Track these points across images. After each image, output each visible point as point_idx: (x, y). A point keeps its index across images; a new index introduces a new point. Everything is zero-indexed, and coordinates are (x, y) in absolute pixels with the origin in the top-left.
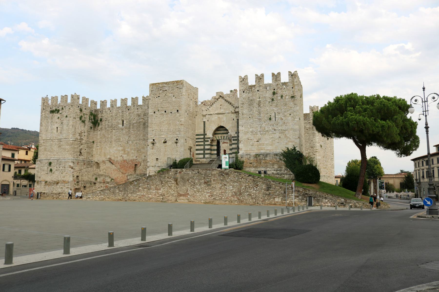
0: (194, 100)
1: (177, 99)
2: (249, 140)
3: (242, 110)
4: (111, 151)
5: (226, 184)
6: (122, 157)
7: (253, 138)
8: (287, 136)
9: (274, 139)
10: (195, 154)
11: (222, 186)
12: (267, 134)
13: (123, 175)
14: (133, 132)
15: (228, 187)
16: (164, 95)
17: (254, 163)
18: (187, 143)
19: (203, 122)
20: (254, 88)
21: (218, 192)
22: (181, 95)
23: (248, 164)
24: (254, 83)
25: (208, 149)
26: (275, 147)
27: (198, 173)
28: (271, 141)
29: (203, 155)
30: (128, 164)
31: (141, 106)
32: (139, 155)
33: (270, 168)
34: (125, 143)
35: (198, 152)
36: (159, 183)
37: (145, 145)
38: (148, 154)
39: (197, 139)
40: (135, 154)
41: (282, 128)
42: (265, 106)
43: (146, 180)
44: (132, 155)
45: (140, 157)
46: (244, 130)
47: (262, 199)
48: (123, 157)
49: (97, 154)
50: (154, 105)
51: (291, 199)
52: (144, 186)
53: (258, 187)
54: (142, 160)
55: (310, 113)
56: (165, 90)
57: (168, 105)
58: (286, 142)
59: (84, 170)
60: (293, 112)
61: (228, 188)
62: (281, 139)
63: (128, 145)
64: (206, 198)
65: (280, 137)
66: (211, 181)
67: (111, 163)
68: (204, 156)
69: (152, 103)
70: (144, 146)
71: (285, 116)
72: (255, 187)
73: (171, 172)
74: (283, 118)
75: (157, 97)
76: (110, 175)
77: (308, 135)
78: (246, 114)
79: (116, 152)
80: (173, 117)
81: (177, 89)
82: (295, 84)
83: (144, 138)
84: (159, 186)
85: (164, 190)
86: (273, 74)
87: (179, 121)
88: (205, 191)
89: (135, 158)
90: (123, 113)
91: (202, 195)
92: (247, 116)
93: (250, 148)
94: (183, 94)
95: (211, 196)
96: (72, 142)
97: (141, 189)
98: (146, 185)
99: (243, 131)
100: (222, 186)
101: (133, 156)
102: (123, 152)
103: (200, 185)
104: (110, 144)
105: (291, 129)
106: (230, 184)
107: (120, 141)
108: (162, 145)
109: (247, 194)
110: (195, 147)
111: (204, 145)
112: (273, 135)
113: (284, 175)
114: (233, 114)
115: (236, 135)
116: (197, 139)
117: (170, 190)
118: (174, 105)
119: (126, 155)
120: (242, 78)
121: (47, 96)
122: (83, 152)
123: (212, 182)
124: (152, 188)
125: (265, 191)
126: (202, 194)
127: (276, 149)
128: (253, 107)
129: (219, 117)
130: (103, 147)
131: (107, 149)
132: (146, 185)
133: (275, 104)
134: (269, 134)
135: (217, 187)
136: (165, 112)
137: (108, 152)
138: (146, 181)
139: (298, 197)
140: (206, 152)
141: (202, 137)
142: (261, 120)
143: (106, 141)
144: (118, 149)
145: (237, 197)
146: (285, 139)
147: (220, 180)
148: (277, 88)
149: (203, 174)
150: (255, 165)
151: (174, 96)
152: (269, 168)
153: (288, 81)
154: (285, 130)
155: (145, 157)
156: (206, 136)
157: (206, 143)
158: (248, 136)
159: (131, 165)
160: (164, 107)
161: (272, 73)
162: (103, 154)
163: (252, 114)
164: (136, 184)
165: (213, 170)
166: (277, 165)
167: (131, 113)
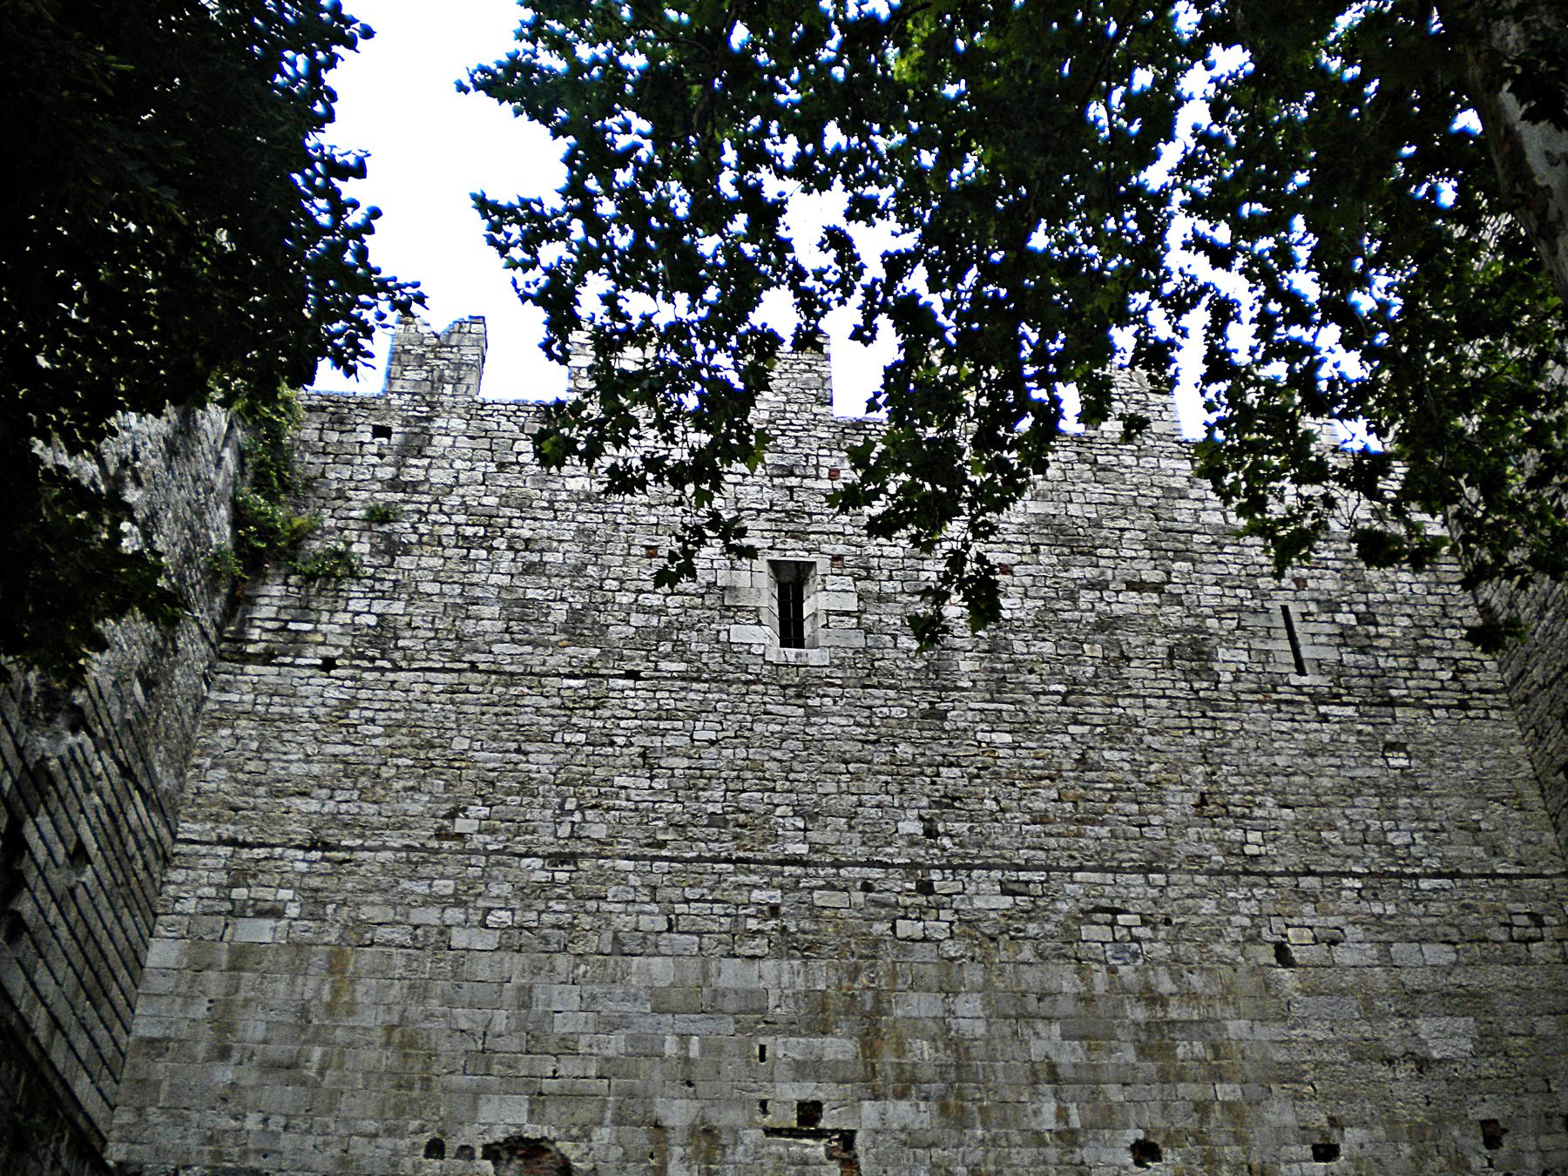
6: (817, 1149)
14: (1008, 738)
34: (867, 887)
40: (1115, 1093)
44: (1049, 1108)
45: (1231, 1152)
48: (847, 1138)
49: (224, 1053)
63: (939, 929)
70: (1256, 970)
79: (671, 1047)
90: (791, 489)
101: (1069, 1138)
102: (839, 1047)
104: (529, 893)
107: (769, 851)
130: (383, 933)
131: (483, 968)
137: (501, 1020)
143: (461, 825)
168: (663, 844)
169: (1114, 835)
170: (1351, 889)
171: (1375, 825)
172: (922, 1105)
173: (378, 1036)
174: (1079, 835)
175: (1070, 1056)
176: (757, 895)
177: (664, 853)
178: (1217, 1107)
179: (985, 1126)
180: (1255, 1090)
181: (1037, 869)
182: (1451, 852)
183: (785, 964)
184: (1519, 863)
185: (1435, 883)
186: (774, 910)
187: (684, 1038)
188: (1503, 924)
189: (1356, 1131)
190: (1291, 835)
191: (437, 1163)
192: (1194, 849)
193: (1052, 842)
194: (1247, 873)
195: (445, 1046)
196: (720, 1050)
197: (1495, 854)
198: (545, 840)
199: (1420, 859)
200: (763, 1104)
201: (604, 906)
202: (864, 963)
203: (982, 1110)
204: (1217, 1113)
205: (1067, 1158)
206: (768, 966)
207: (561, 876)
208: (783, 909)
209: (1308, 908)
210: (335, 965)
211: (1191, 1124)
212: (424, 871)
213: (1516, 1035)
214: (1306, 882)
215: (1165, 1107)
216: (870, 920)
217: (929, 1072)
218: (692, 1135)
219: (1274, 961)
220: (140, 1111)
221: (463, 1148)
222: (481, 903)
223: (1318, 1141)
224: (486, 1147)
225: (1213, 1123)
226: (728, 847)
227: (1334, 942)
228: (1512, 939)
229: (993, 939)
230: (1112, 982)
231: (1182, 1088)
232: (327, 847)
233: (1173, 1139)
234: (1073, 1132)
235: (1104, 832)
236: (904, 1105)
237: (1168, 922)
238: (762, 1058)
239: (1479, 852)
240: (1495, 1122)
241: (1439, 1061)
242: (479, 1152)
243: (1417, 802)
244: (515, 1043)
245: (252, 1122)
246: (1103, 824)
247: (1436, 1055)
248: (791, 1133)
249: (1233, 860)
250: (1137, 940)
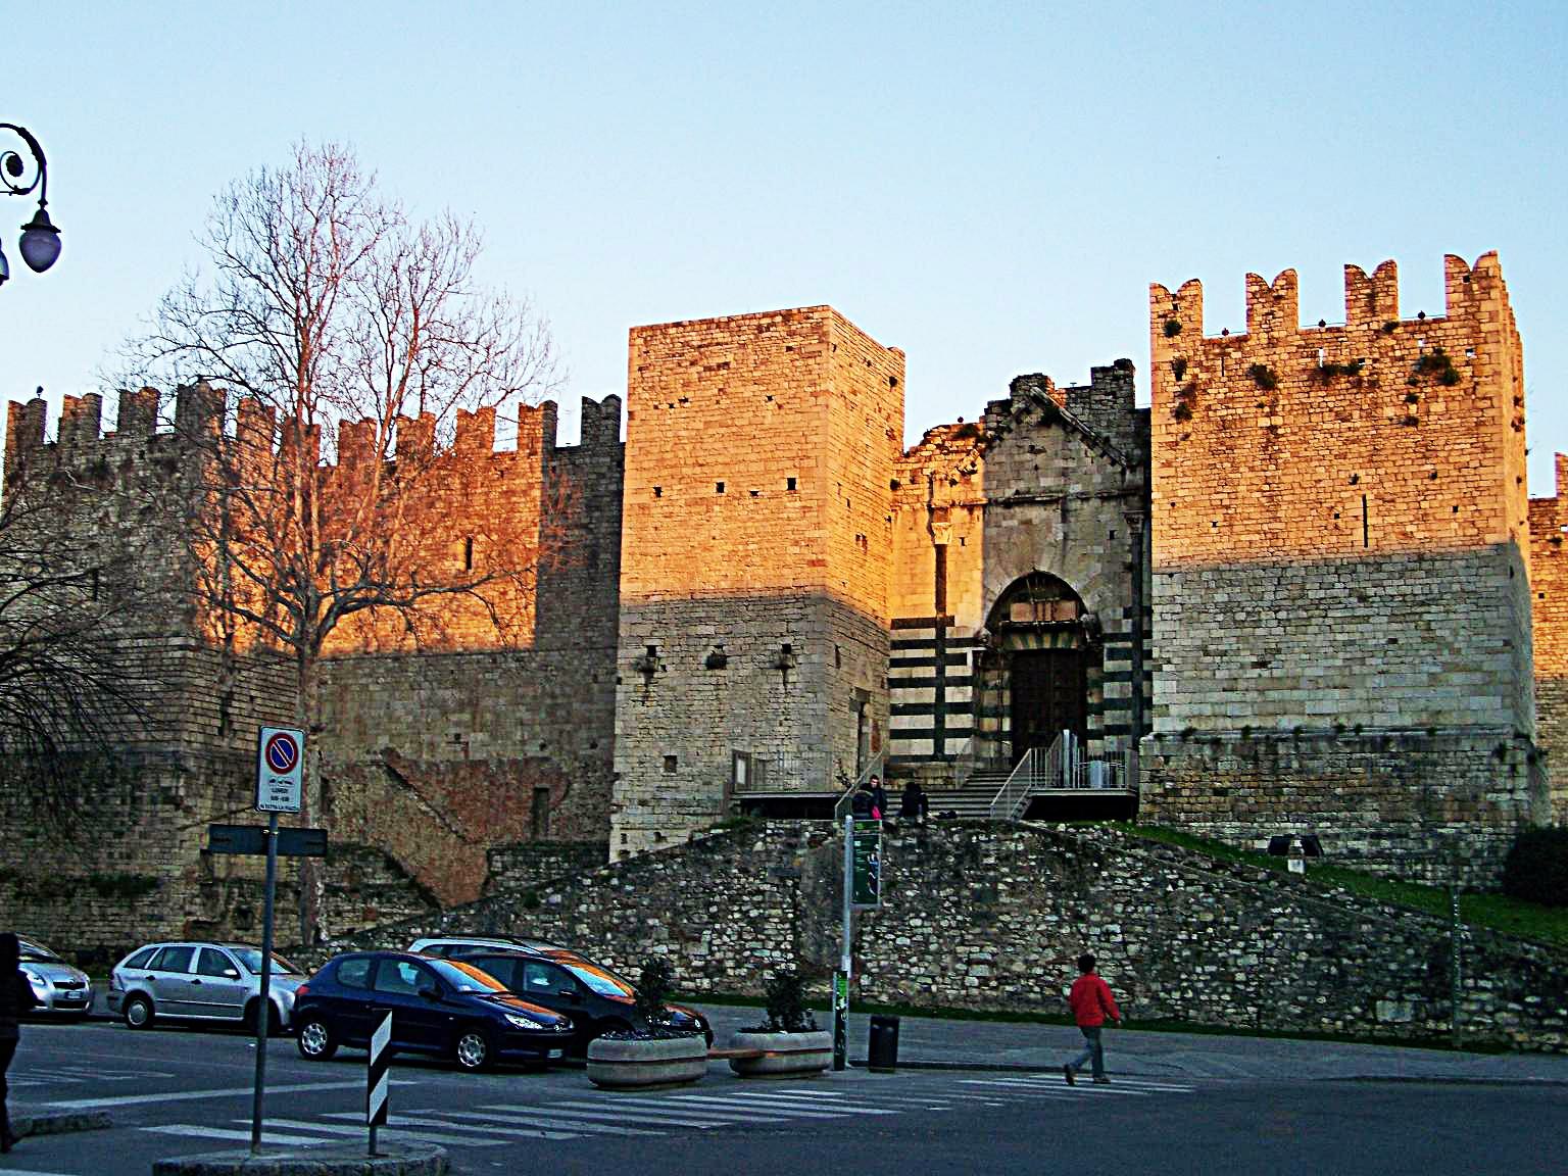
0: (879, 418)
1: (790, 418)
2: (1208, 659)
3: (1172, 480)
4: (400, 713)
5: (1084, 911)
6: (458, 747)
7: (1235, 647)
8: (1438, 633)
9: (1359, 655)
10: (884, 735)
11: (1059, 925)
12: (1314, 621)
15: (1097, 931)
16: (709, 393)
17: (1241, 792)
18: (844, 668)
19: (933, 550)
20: (1238, 355)
21: (1037, 957)
22: (815, 395)
23: (1206, 799)
24: (1239, 328)
25: (959, 708)
26: (1365, 696)
27: (922, 843)
28: (1339, 663)
29: (931, 741)
30: (492, 783)
31: (571, 450)
32: (561, 732)
33: (1337, 819)
34: (478, 662)
35: (904, 722)
36: (689, 903)
37: (595, 676)
38: (618, 731)
39: (896, 645)
40: (537, 728)
41: (1408, 590)
42: (1309, 460)
43: (615, 882)
45: (567, 747)
46: (1179, 600)
47: (1296, 1003)
50: (656, 450)
51: (1473, 1007)
52: (607, 918)
53: (1276, 936)
54: (577, 764)
55: (1560, 494)
56: (719, 366)
57: (732, 451)
58: (1434, 669)
59: (244, 815)
60: (1476, 494)
61: (1094, 938)
62: (1400, 653)
64: (963, 992)
65: (1394, 641)
66: (996, 893)
67: (399, 777)
68: (939, 747)
69: (642, 436)
71: (1426, 515)
72: (1255, 931)
73: (760, 839)
74: (1409, 528)
75: (671, 406)
76: (387, 849)
77: (1543, 625)
78: (1193, 505)
80: (767, 520)
81: (787, 357)
82: (1484, 328)
83: (588, 639)
84: (689, 919)
85: (717, 942)
86: (1353, 276)
87: (796, 543)
88: (960, 949)
89: (533, 750)
91: (943, 976)
92: (1199, 519)
93: (1212, 704)
94: (823, 387)
95: (993, 983)
96: (178, 654)
97: (587, 931)
98: (616, 913)
99: (1172, 600)
100: (1059, 925)
101: (523, 742)
102: (466, 717)
103: (929, 915)
104: (388, 671)
105: (1463, 591)
106: (1109, 912)
108: (701, 679)
109: (1210, 973)
110: (889, 696)
111: (941, 683)
112: (1353, 627)
113: (1419, 867)
114: (1110, 506)
115: (1127, 627)
116: (896, 645)
117: (758, 940)
118: (773, 448)
119: (480, 736)
120: (1167, 294)
121: (40, 390)
122: (237, 711)
123: (1004, 899)
124: (652, 927)
125: (1315, 960)
126: (944, 969)
127: (1371, 712)
128: (1235, 468)
129: (1028, 522)
131: (377, 696)
132: (615, 909)
133: (1363, 449)
134: (1329, 621)
135: (1029, 928)
136: (720, 487)
138: (614, 889)
139: (1518, 998)
140: (952, 721)
141: (930, 634)
142: (1280, 543)
145: (1149, 990)
146: (1422, 653)
147: (1049, 889)
148: (1376, 356)
149: (948, 853)
150: (1243, 806)
151: (770, 398)
152: (1327, 820)
153: (1442, 313)
154: (1422, 598)
155: (594, 746)
156: (949, 632)
157: (951, 671)
158: (1203, 634)
159: (512, 793)
160: (710, 460)
161: (1347, 267)
162: (351, 726)
163: (1228, 507)
164: (557, 904)
165: (1009, 828)
166: (1375, 805)
167: (514, 493)
175: (527, 716)
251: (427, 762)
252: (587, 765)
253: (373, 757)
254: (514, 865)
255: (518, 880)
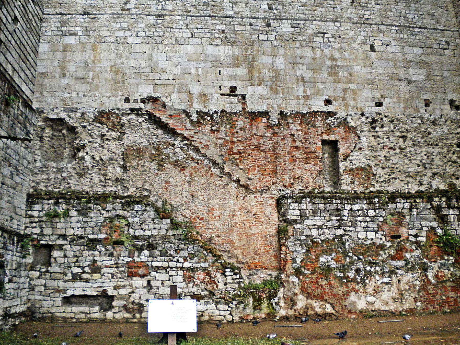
6: (235, 99)
13: (251, 199)
30: (274, 134)
40: (320, 85)
44: (301, 89)
45: (352, 103)
48: (244, 97)
49: (64, 75)
54: (363, 119)
63: (272, 37)
79: (193, 71)
101: (306, 98)
102: (242, 71)
104: (150, 26)
107: (222, 13)
130: (107, 39)
143: (128, 6)
144: (208, 52)
159: (298, 143)
162: (108, 75)
168: (190, 11)
169: (325, 11)
170: (395, 30)
171: (404, 12)
172: (265, 88)
173: (108, 69)
174: (315, 10)
175: (308, 75)
176: (218, 27)
177: (190, 14)
178: (349, 90)
179: (283, 94)
180: (360, 86)
181: (302, 20)
182: (425, 21)
183: (226, 47)
184: (444, 26)
185: (419, 30)
186: (223, 32)
187: (197, 68)
188: (438, 44)
189: (388, 99)
190: (378, 13)
191: (128, 104)
192: (349, 16)
193: (307, 12)
194: (364, 23)
195: (128, 71)
196: (207, 71)
197: (438, 23)
198: (154, 10)
199: (416, 23)
200: (220, 87)
201: (172, 30)
202: (250, 47)
203: (282, 89)
204: (349, 92)
205: (305, 103)
206: (221, 48)
207: (159, 21)
208: (226, 31)
209: (381, 35)
210: (94, 49)
211: (341, 95)
212: (118, 20)
213: (437, 76)
214: (381, 27)
215: (334, 90)
216: (251, 34)
217: (267, 78)
218: (200, 95)
219: (370, 50)
220: (41, 93)
221: (135, 100)
222: (136, 30)
223: (377, 101)
224: (141, 99)
225: (348, 95)
226: (209, 12)
227: (388, 45)
228: (439, 48)
229: (288, 41)
230: (322, 54)
231: (340, 85)
232: (88, 14)
233: (336, 99)
234: (308, 96)
235: (323, 9)
236: (260, 88)
237: (340, 37)
238: (220, 74)
239: (433, 22)
240: (428, 99)
241: (415, 81)
242: (139, 101)
243: (416, 5)
244: (148, 70)
245: (74, 94)
246: (323, 7)
247: (414, 79)
248: (228, 95)
249: (360, 19)
250: (330, 42)
251: (198, 112)
252: (374, 121)
253: (134, 106)
254: (314, 213)
255: (319, 228)
